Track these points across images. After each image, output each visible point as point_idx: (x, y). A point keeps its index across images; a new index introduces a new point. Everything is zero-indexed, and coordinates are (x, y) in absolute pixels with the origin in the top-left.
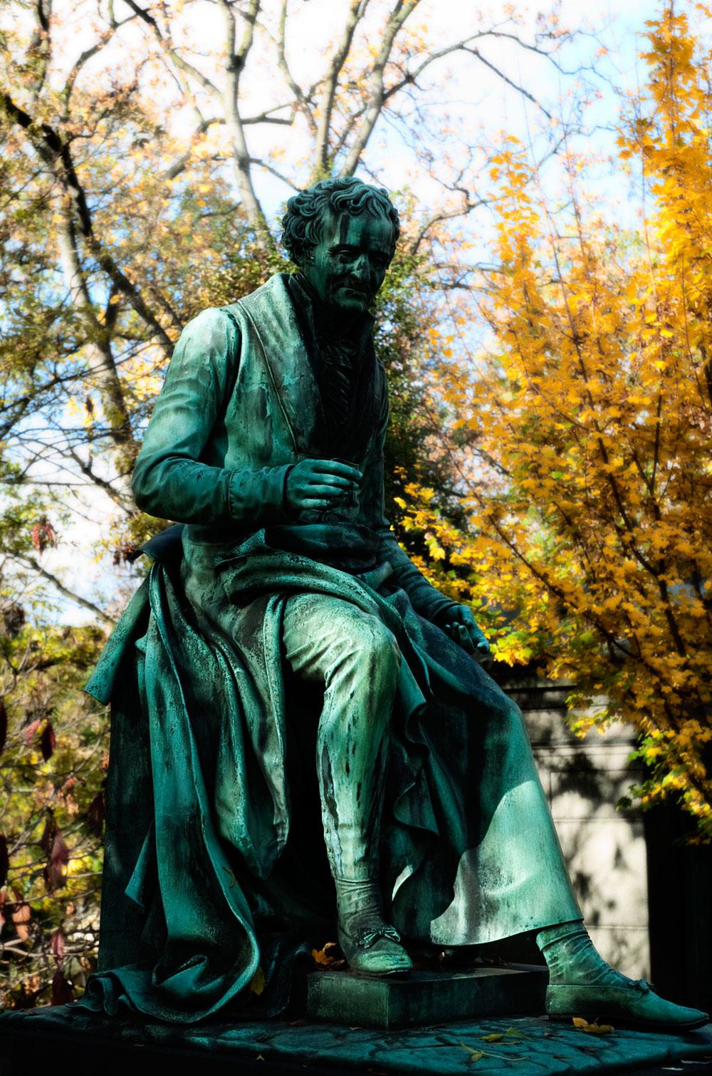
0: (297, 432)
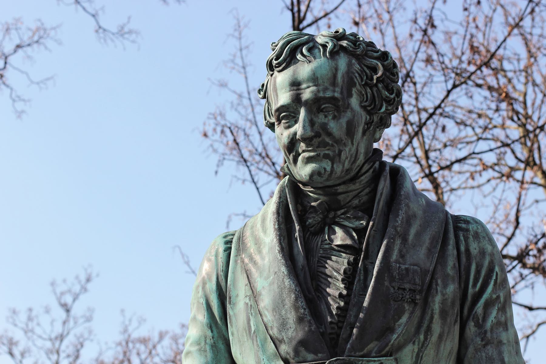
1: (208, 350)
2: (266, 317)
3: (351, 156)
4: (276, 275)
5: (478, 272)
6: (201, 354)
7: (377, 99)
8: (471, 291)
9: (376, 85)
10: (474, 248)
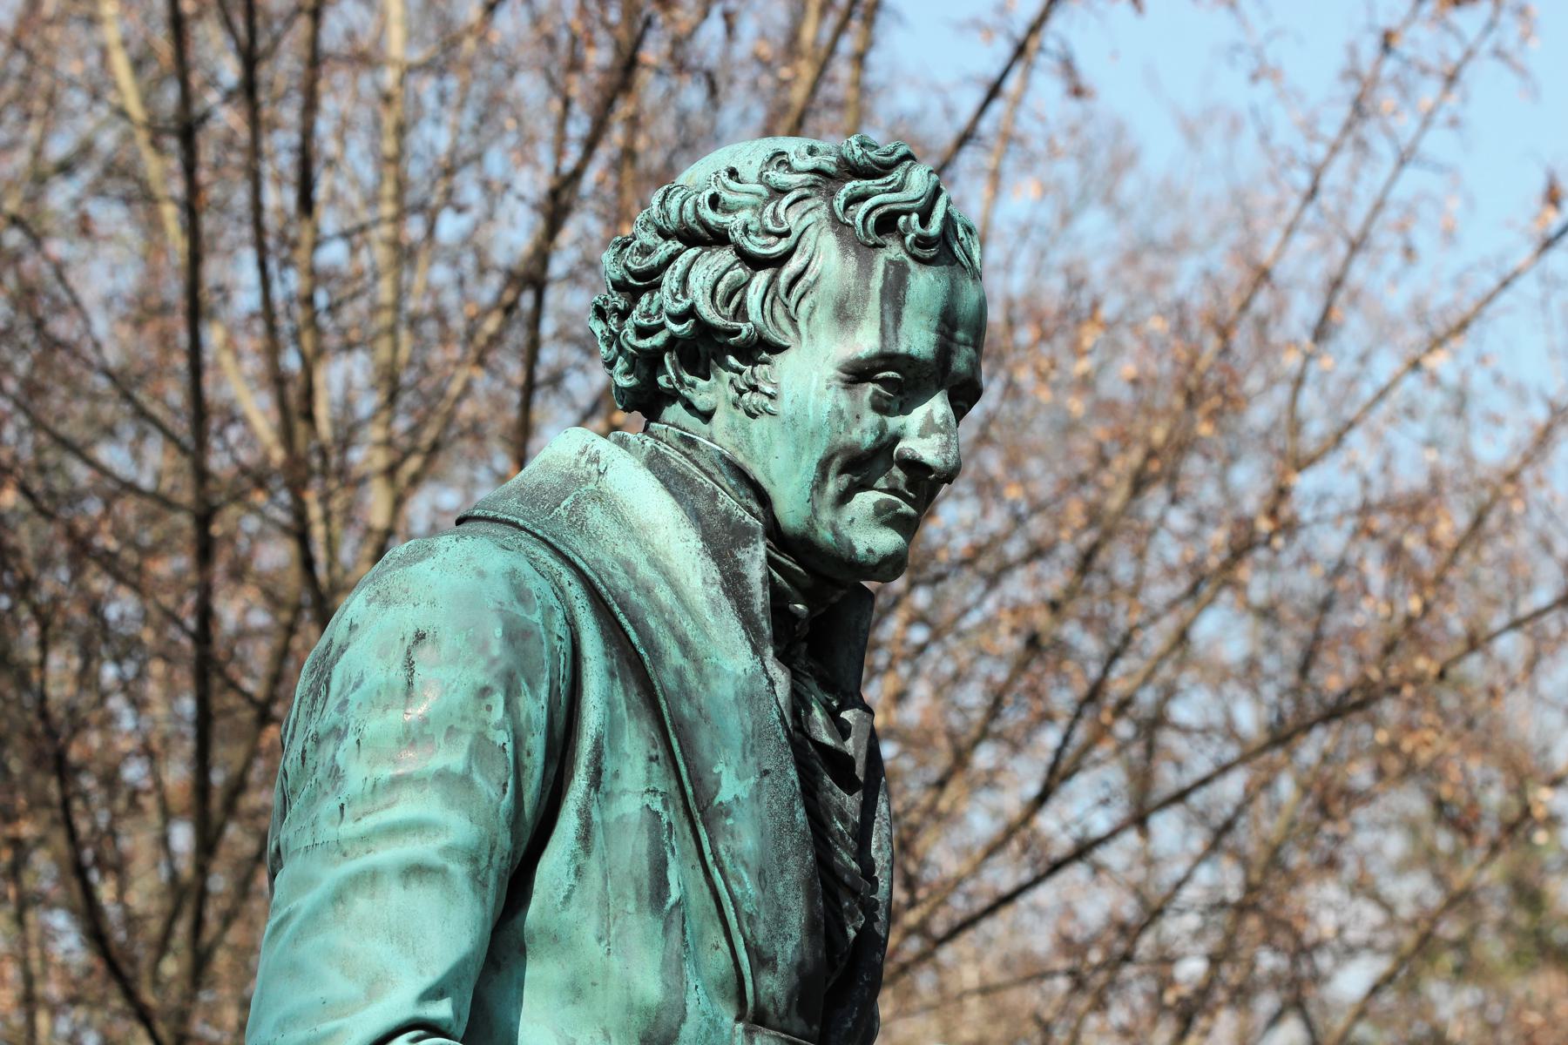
0: (763, 962)
1: (491, 886)
2: (740, 882)
4: (767, 780)
6: (474, 891)
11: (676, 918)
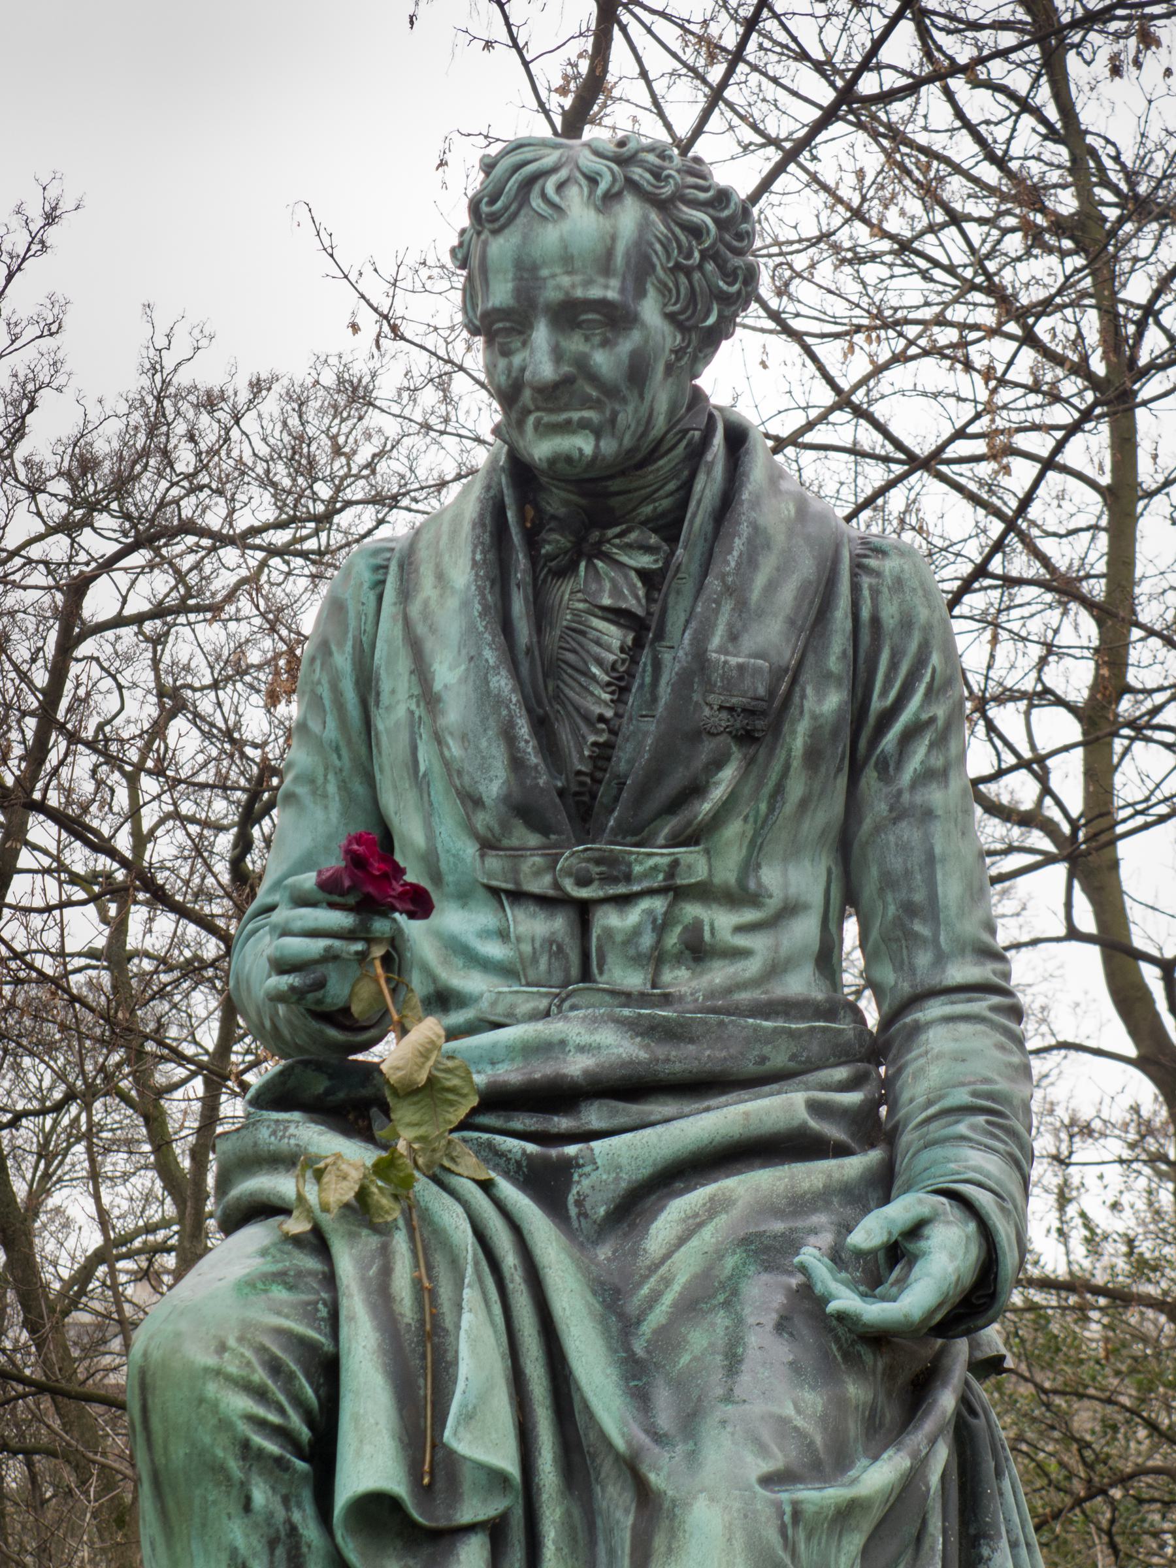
2: (449, 748)
3: (638, 423)
5: (894, 666)
7: (699, 299)
8: (877, 704)
9: (700, 267)
10: (890, 612)
11: (425, 786)
